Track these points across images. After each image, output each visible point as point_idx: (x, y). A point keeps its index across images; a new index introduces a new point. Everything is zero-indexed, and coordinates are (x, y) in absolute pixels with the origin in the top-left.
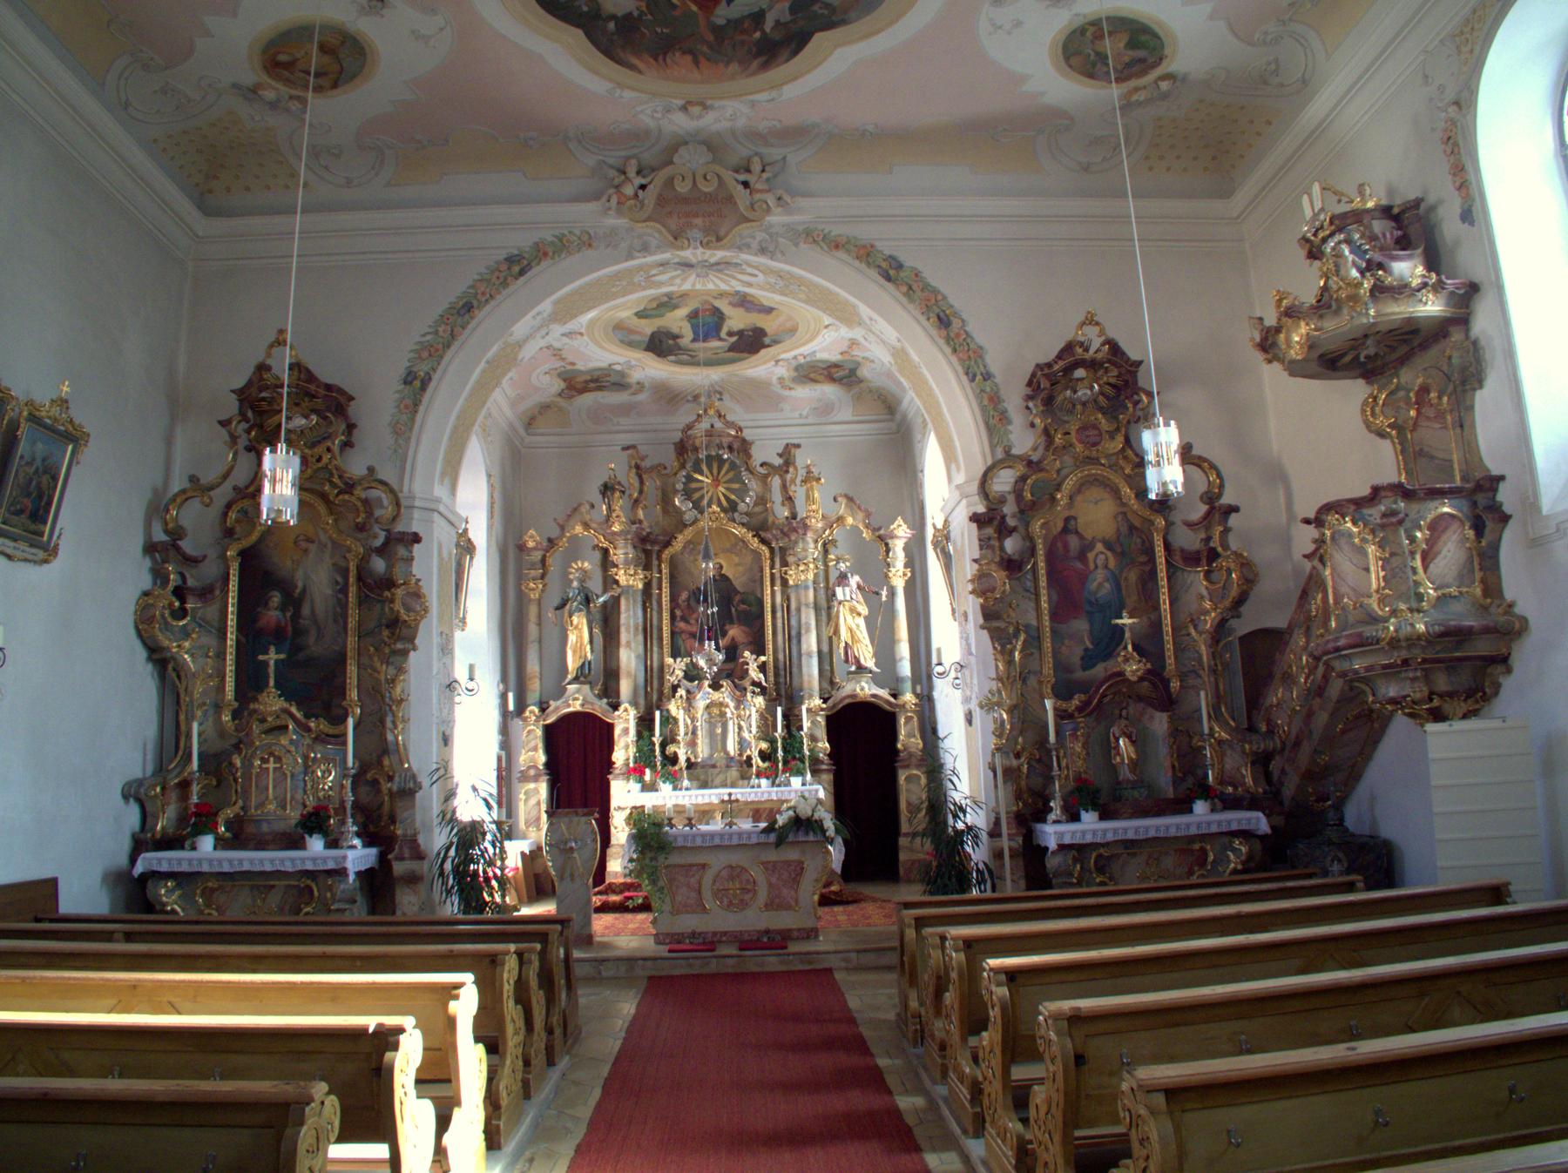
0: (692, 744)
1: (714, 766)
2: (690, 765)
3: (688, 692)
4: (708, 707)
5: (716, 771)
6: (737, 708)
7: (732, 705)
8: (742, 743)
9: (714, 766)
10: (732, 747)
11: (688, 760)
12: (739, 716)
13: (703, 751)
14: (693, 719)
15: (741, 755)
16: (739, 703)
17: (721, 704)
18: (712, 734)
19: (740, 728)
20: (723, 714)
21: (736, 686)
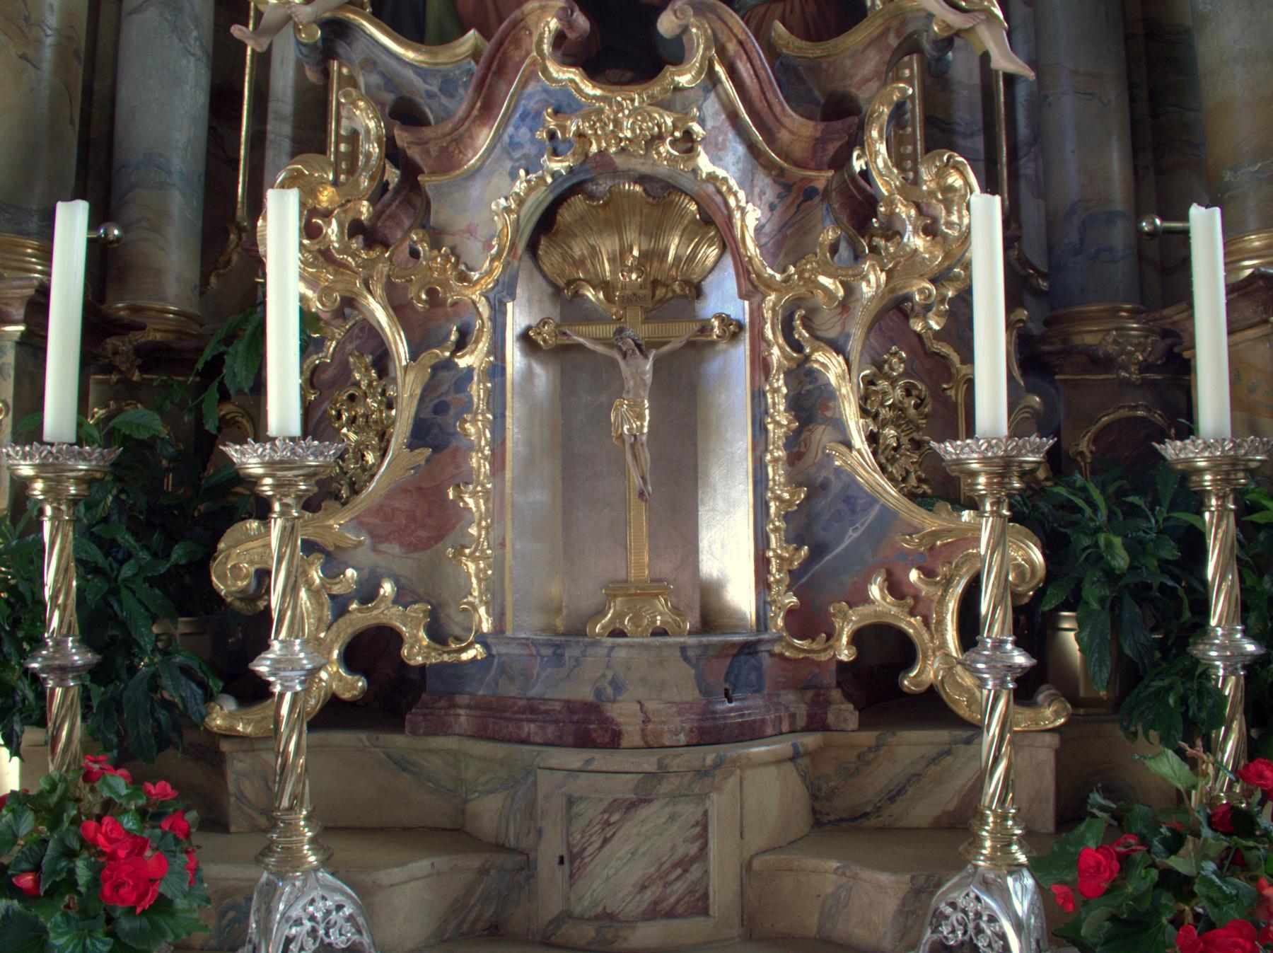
0: (426, 517)
1: (589, 728)
2: (387, 689)
3: (405, 113)
4: (546, 224)
5: (616, 771)
6: (789, 240)
7: (751, 217)
8: (810, 526)
9: (589, 728)
10: (728, 552)
11: (371, 650)
12: (799, 319)
13: (498, 578)
14: (430, 323)
15: (807, 621)
16: (830, 204)
17: (662, 193)
18: (575, 443)
19: (810, 402)
20: (676, 294)
21: (789, 74)
